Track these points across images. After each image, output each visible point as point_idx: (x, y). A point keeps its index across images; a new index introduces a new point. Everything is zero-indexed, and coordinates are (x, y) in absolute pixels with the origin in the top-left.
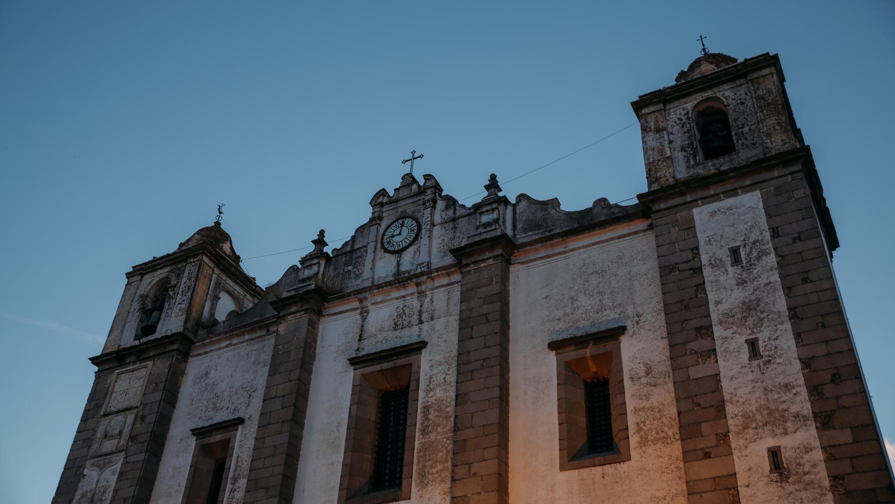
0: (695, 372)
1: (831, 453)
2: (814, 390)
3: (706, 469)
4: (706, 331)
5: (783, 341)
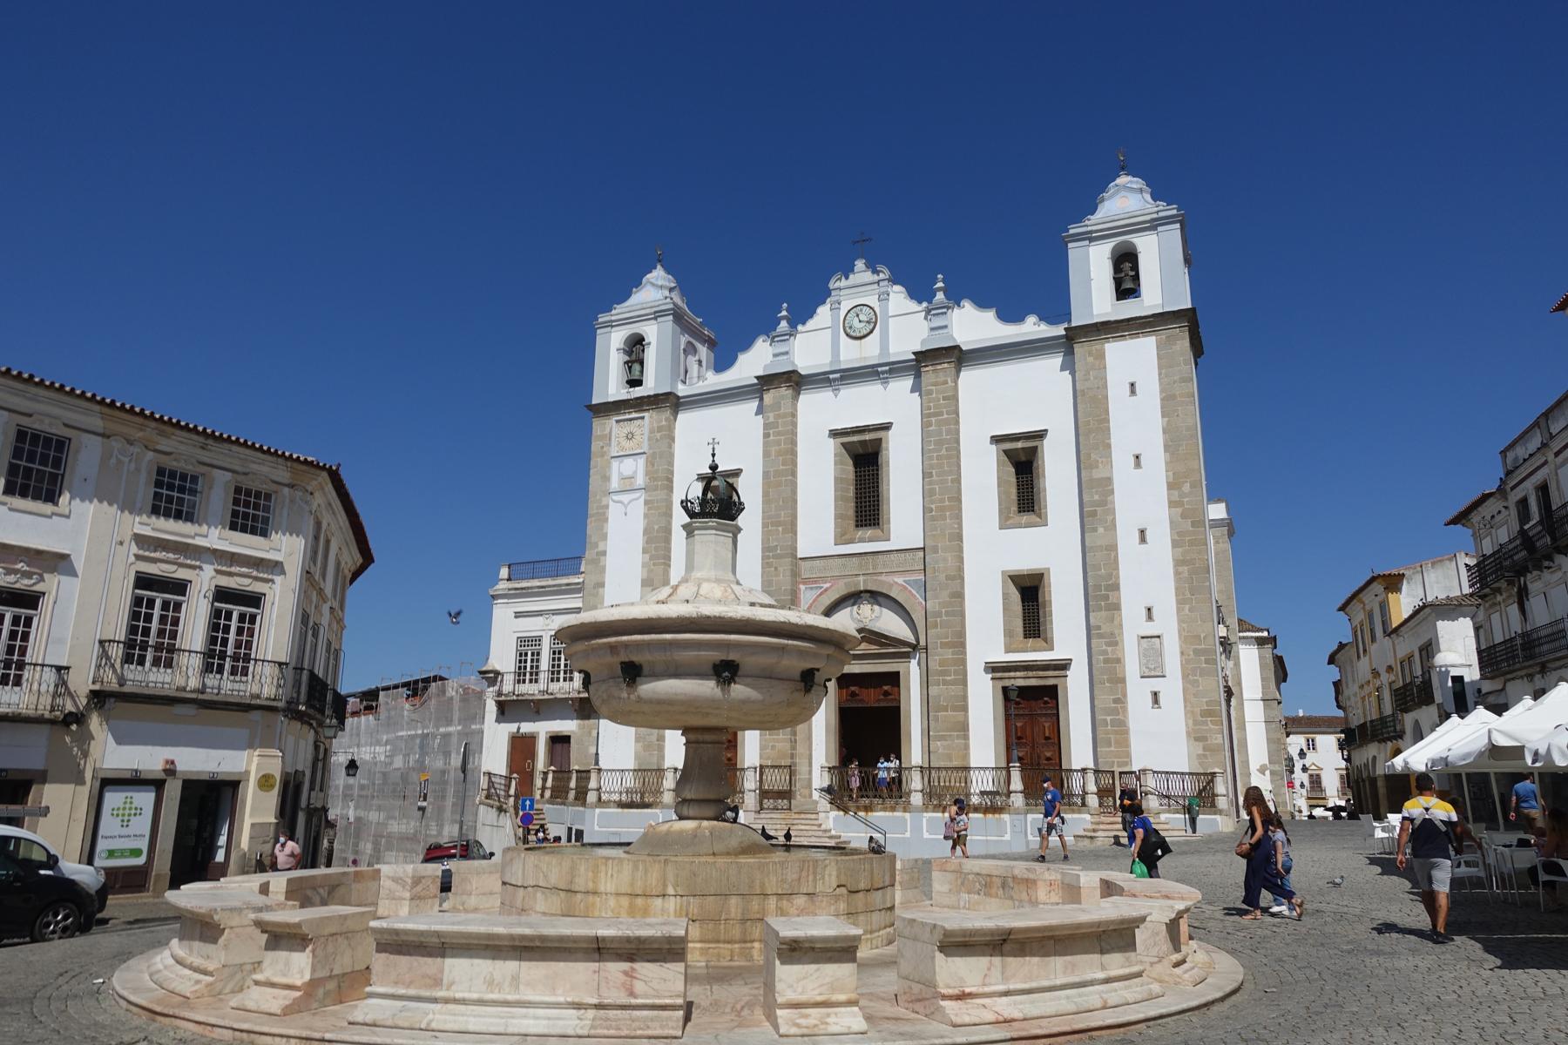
0: (1098, 474)
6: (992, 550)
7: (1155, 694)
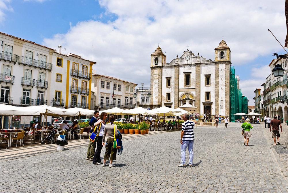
0: (217, 80)
1: (226, 88)
2: (226, 84)
3: (217, 88)
4: (218, 77)
5: (224, 79)
6: (204, 89)
7: (222, 107)
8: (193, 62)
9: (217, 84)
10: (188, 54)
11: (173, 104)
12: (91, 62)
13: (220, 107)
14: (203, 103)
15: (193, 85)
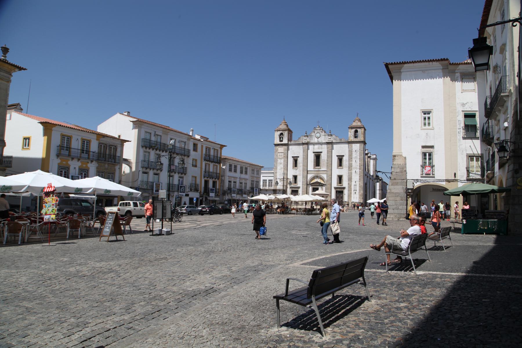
3: (350, 172)
4: (352, 158)
6: (336, 172)
8: (324, 140)
9: (350, 167)
10: (319, 131)
11: (301, 188)
12: (221, 145)
13: (353, 192)
14: (335, 188)
15: (323, 167)
